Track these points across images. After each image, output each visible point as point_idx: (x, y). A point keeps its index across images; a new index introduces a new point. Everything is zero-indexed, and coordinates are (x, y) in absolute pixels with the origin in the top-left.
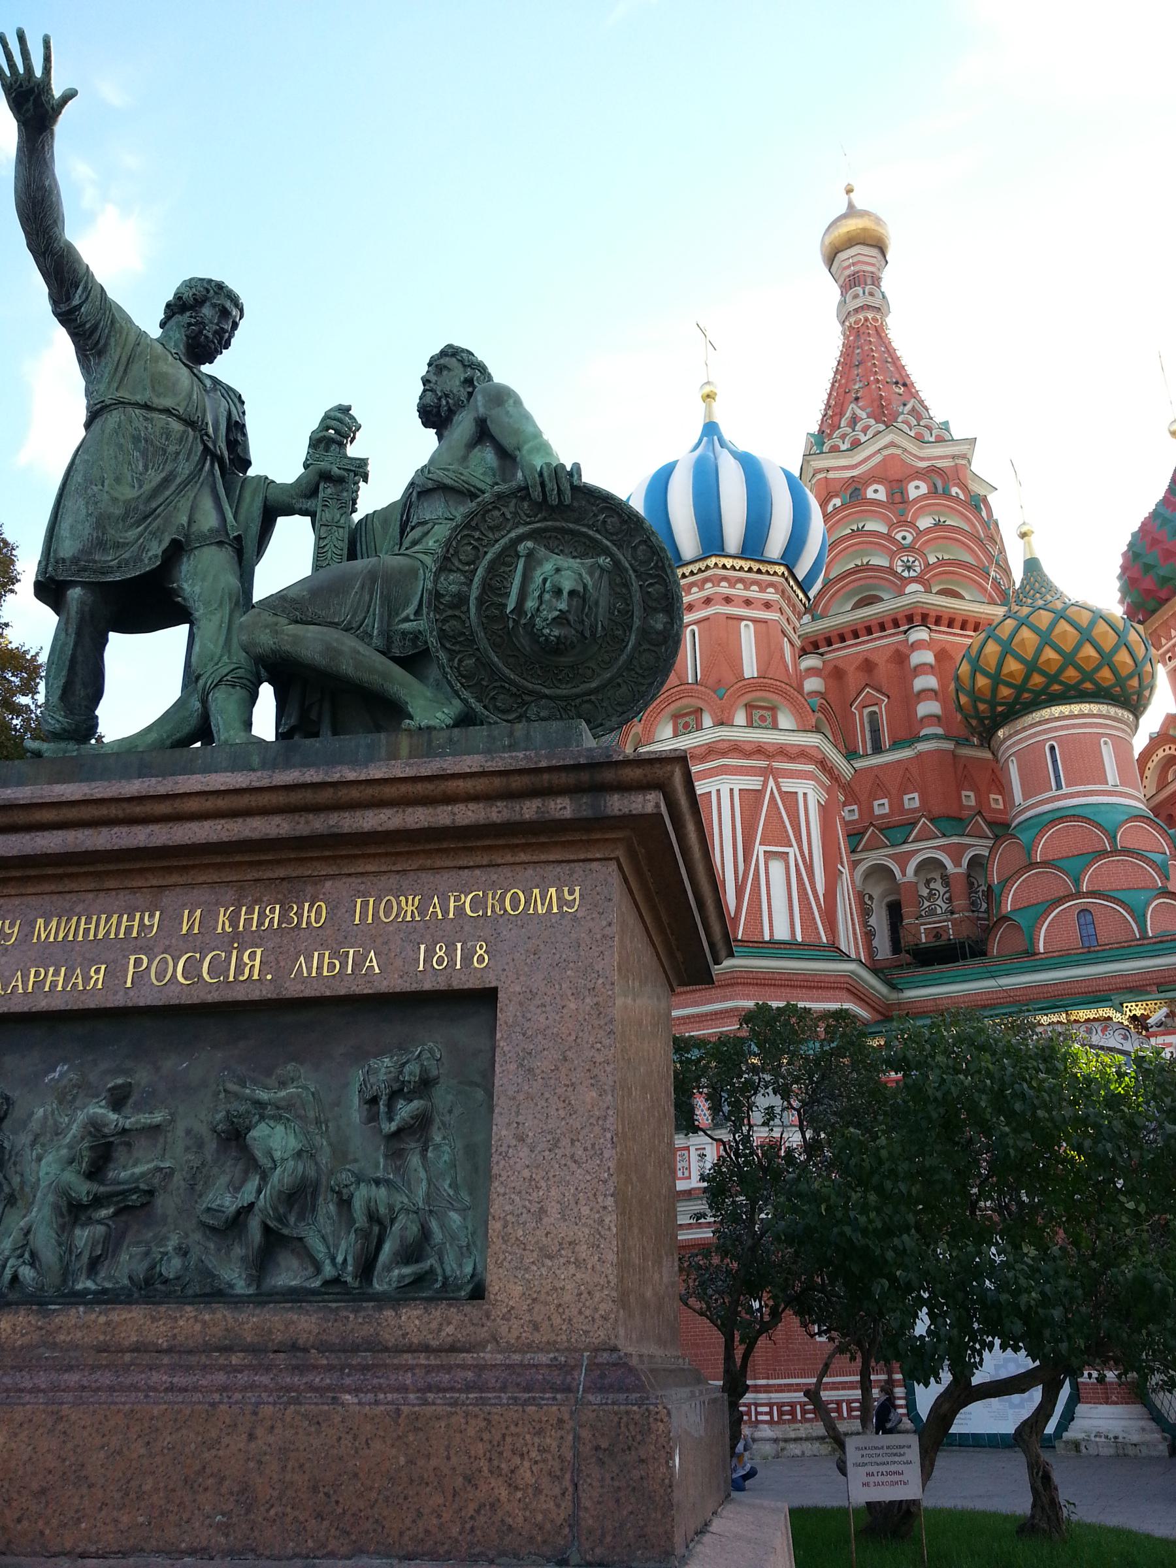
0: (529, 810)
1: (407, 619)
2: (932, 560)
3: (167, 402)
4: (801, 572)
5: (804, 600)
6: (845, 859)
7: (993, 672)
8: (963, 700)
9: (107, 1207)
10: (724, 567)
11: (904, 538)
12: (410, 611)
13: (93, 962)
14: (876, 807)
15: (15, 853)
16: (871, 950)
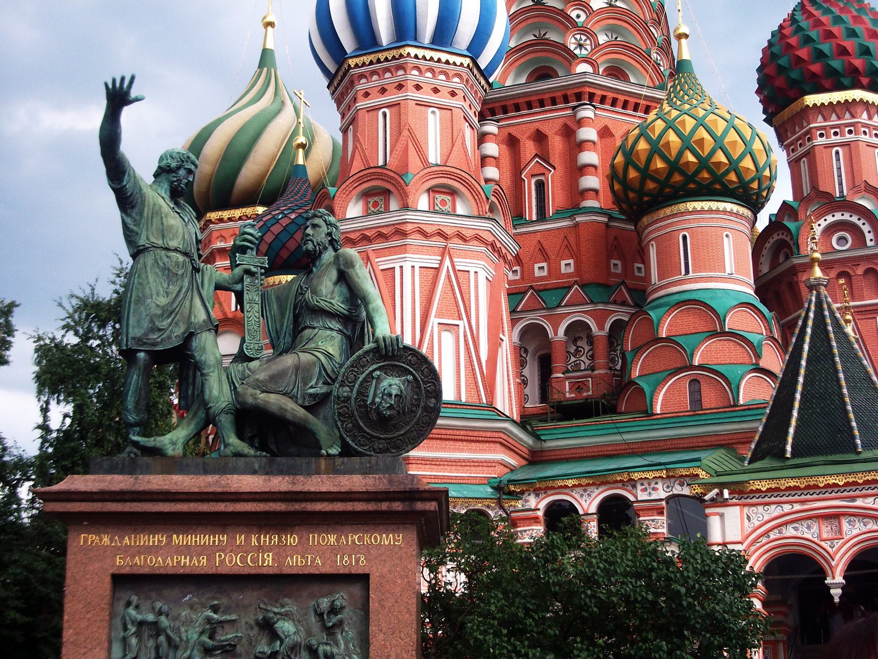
0: (384, 506)
1: (312, 387)
2: (602, 39)
3: (173, 244)
4: (483, 62)
5: (486, 86)
6: (506, 329)
7: (642, 167)
8: (617, 187)
9: (218, 650)
10: (416, 57)
11: (578, 16)
12: (313, 383)
13: (199, 555)
14: (536, 269)
15: (167, 510)
16: (523, 398)
